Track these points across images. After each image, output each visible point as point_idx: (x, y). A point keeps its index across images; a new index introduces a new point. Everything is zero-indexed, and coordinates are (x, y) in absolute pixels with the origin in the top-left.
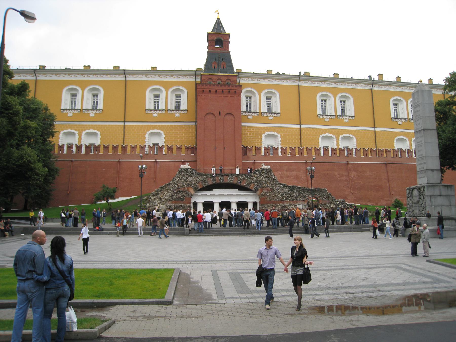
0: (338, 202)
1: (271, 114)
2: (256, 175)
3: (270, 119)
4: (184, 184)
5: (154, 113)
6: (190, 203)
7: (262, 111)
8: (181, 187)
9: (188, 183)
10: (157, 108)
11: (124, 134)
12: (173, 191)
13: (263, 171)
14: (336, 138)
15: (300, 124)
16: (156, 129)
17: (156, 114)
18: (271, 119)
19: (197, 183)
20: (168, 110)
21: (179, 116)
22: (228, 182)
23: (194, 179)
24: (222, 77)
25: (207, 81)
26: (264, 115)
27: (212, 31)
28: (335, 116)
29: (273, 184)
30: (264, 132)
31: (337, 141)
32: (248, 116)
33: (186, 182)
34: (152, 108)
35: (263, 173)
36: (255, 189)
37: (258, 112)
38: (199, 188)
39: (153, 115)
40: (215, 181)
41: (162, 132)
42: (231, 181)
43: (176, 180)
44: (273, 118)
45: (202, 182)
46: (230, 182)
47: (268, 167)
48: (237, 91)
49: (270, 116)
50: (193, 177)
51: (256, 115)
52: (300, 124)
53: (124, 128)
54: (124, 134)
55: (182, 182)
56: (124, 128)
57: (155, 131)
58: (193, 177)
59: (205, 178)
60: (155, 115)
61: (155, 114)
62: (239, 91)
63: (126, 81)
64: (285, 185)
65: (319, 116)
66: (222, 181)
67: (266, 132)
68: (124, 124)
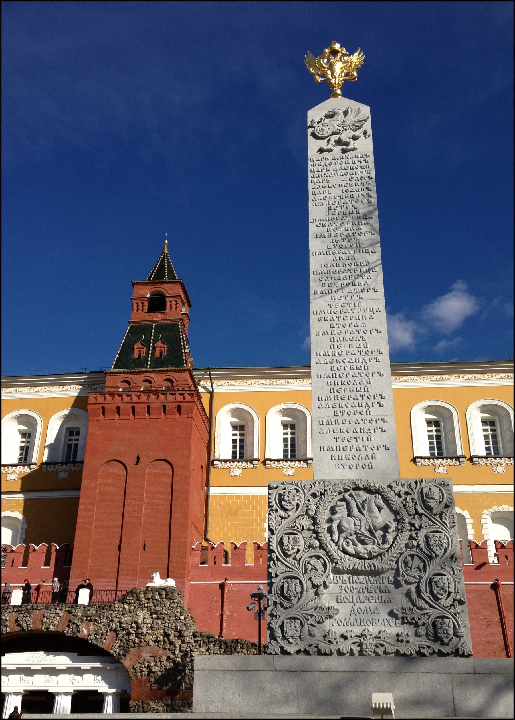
2: (126, 606)
3: (287, 474)
5: (11, 473)
7: (267, 457)
13: (150, 595)
14: (472, 516)
17: (15, 473)
22: (43, 627)
28: (465, 458)
29: (171, 633)
31: (474, 526)
32: (232, 470)
37: (256, 460)
39: (9, 475)
42: (52, 628)
44: (296, 473)
47: (171, 582)
51: (252, 466)
64: (208, 637)
66: (25, 626)
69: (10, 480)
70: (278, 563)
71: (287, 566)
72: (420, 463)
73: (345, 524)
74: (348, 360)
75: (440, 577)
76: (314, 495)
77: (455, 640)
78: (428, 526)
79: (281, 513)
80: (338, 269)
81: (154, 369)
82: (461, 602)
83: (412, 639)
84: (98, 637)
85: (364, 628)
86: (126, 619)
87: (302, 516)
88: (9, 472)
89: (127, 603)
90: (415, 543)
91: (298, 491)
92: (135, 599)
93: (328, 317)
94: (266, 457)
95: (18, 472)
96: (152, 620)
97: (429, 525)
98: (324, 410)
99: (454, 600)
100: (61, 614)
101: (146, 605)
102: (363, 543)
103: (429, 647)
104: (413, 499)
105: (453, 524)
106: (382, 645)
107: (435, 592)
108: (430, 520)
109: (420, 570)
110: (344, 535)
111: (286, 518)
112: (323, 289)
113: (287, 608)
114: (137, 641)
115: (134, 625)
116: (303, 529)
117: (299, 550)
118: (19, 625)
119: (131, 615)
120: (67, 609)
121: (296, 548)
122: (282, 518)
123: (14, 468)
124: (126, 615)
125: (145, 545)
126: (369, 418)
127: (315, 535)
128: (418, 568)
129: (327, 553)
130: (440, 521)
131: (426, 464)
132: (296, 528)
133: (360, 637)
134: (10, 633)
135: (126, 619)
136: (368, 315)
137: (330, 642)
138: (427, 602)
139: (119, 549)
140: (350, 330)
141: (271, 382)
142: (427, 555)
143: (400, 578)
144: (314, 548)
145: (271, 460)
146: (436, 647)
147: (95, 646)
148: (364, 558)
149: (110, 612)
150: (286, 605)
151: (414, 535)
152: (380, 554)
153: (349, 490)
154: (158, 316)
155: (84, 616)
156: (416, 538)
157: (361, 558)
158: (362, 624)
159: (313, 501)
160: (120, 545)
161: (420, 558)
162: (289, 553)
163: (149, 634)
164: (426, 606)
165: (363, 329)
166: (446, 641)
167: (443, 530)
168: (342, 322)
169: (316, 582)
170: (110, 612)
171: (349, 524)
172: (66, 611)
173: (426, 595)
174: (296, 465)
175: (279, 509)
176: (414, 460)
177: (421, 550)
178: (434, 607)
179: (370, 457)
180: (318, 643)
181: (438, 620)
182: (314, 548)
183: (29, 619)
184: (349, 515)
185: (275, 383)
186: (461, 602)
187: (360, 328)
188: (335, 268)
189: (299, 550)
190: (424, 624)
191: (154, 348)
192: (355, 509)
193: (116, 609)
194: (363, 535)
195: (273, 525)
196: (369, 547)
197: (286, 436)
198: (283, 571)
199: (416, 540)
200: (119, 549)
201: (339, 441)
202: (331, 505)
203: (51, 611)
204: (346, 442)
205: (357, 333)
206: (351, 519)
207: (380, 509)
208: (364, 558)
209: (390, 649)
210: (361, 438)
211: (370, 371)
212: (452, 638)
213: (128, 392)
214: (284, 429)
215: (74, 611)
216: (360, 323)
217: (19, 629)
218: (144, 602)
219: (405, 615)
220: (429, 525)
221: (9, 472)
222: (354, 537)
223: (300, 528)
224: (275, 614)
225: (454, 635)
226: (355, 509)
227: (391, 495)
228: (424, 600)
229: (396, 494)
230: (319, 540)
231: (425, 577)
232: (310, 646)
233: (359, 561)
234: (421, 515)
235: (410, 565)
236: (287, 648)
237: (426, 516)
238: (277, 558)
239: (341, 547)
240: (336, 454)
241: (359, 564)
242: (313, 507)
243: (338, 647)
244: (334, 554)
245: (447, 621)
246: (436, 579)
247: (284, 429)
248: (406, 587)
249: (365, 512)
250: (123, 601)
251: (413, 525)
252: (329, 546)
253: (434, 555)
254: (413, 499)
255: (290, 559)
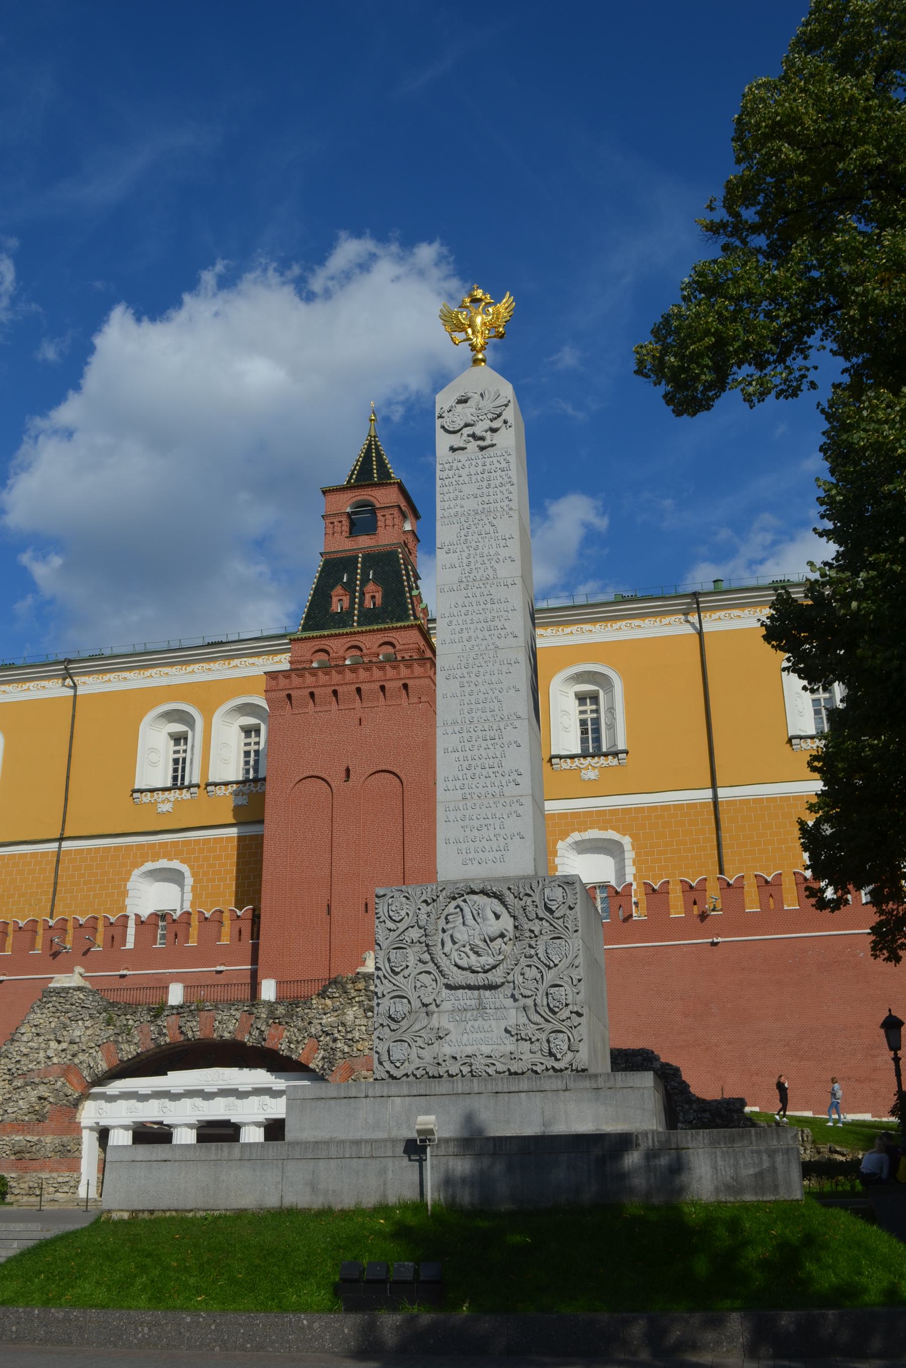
0: (707, 1115)
1: (589, 759)
2: (328, 1002)
3: (586, 777)
4: (51, 1053)
5: (163, 802)
6: (77, 1129)
8: (38, 1067)
9: (64, 1045)
10: (178, 783)
11: (56, 883)
12: (10, 1082)
13: (361, 985)
15: (714, 787)
16: (164, 857)
17: (169, 801)
18: (593, 777)
19: (99, 1046)
20: (208, 785)
21: (245, 802)
23: (89, 1032)
24: (361, 638)
25: (312, 662)
26: (564, 766)
27: (349, 482)
30: (564, 835)
33: (59, 1042)
34: (169, 784)
35: (360, 990)
36: (320, 1064)
38: (103, 1066)
40: (165, 1035)
41: (185, 868)
42: (227, 1035)
43: (25, 1038)
45: (116, 1042)
46: (222, 1037)
48: (410, 683)
49: (587, 768)
50: (88, 1024)
52: (714, 787)
53: (58, 861)
54: (56, 883)
55: (43, 1045)
56: (58, 861)
57: (163, 863)
58: (88, 1024)
59: (131, 1022)
60: (166, 807)
61: (166, 804)
62: (417, 682)
63: (75, 696)
65: (794, 741)
66: (190, 1034)
67: (573, 831)
68: (60, 847)
69: (163, 813)
70: (385, 982)
71: (394, 985)
72: (799, 746)
73: (457, 936)
74: (480, 727)
75: (557, 988)
76: (425, 901)
77: (570, 1055)
78: (549, 932)
79: (390, 925)
80: (471, 609)
81: (364, 629)
82: (579, 1015)
83: (527, 1056)
84: (292, 1046)
85: (475, 1047)
86: (329, 1020)
87: (412, 927)
88: (160, 800)
89: (329, 998)
90: (533, 952)
91: (408, 898)
92: (340, 991)
93: (459, 673)
94: (553, 753)
95: (173, 799)
96: (366, 1020)
97: (550, 931)
98: (452, 792)
99: (571, 1012)
100: (238, 1015)
101: (357, 999)
102: (477, 953)
103: (542, 1064)
104: (533, 902)
105: (576, 928)
106: (494, 1065)
107: (551, 1006)
108: (551, 925)
109: (537, 982)
110: (456, 946)
111: (394, 931)
112: (452, 636)
113: (394, 1031)
114: (346, 1049)
115: (340, 1028)
116: (412, 942)
117: (407, 966)
118: (182, 1033)
119: (336, 1014)
120: (246, 1009)
121: (404, 964)
122: (390, 930)
123: (167, 793)
124: (329, 1015)
125: (366, 905)
126: (502, 801)
127: (426, 949)
128: (535, 979)
129: (438, 968)
130: (562, 925)
131: (809, 748)
132: (404, 942)
133: (470, 1057)
134: (170, 1044)
135: (329, 1020)
136: (505, 668)
137: (439, 1064)
138: (542, 1017)
139: (329, 913)
140: (483, 689)
141: (554, 631)
142: (545, 965)
143: (516, 993)
144: (425, 963)
145: (560, 757)
146: (550, 1062)
147: (289, 1058)
148: (478, 972)
149: (306, 1011)
150: (394, 1026)
151: (533, 943)
152: (494, 967)
153: (463, 895)
154: (364, 542)
155: (271, 1018)
156: (534, 946)
157: (473, 972)
158: (475, 1043)
159: (425, 909)
160: (329, 906)
161: (538, 968)
162: (397, 970)
163: (363, 1040)
164: (541, 1020)
165: (498, 686)
166: (559, 1056)
167: (564, 935)
168: (474, 679)
169: (426, 1001)
170: (306, 1011)
171: (462, 935)
172: (245, 1011)
173: (544, 1011)
174: (600, 763)
175: (386, 921)
176: (790, 740)
177: (539, 959)
178: (550, 1022)
179: (502, 849)
180: (425, 1065)
181: (551, 1035)
182: (425, 963)
183: (195, 1023)
184: (464, 924)
185: (561, 633)
186: (579, 1015)
187: (495, 686)
188: (468, 608)
189: (407, 966)
190: (538, 1040)
191: (363, 594)
192: (469, 917)
193: (315, 1006)
194: (477, 946)
195: (380, 939)
196: (483, 960)
197: (583, 716)
198: (390, 990)
199: (534, 948)
200: (329, 913)
201: (468, 830)
202: (445, 913)
203: (223, 1011)
204: (475, 832)
205: (490, 692)
206: (464, 929)
207: (497, 917)
208: (478, 972)
209: (500, 1067)
210: (493, 826)
211: (505, 741)
212: (566, 1053)
213: (325, 668)
214: (580, 705)
215: (255, 1011)
216: (494, 679)
217: (182, 1038)
218: (353, 995)
219: (519, 1032)
220: (550, 931)
221: (160, 800)
222: (467, 949)
223: (409, 941)
224: (381, 1037)
225: (569, 1049)
226: (469, 917)
227: (510, 898)
228: (540, 1014)
229: (516, 897)
230: (430, 954)
231: (542, 988)
232: (418, 1068)
233: (472, 975)
234: (541, 919)
235: (526, 977)
236: (394, 1072)
237: (547, 920)
238: (385, 977)
239: (453, 961)
240: (463, 846)
241: (472, 979)
242: (423, 917)
243: (446, 1069)
244: (445, 969)
245: (561, 1035)
246: (552, 990)
247: (580, 705)
248: (523, 1001)
249: (479, 920)
250: (322, 995)
251: (532, 931)
252: (440, 960)
253: (552, 964)
254: (533, 902)
255: (400, 977)
